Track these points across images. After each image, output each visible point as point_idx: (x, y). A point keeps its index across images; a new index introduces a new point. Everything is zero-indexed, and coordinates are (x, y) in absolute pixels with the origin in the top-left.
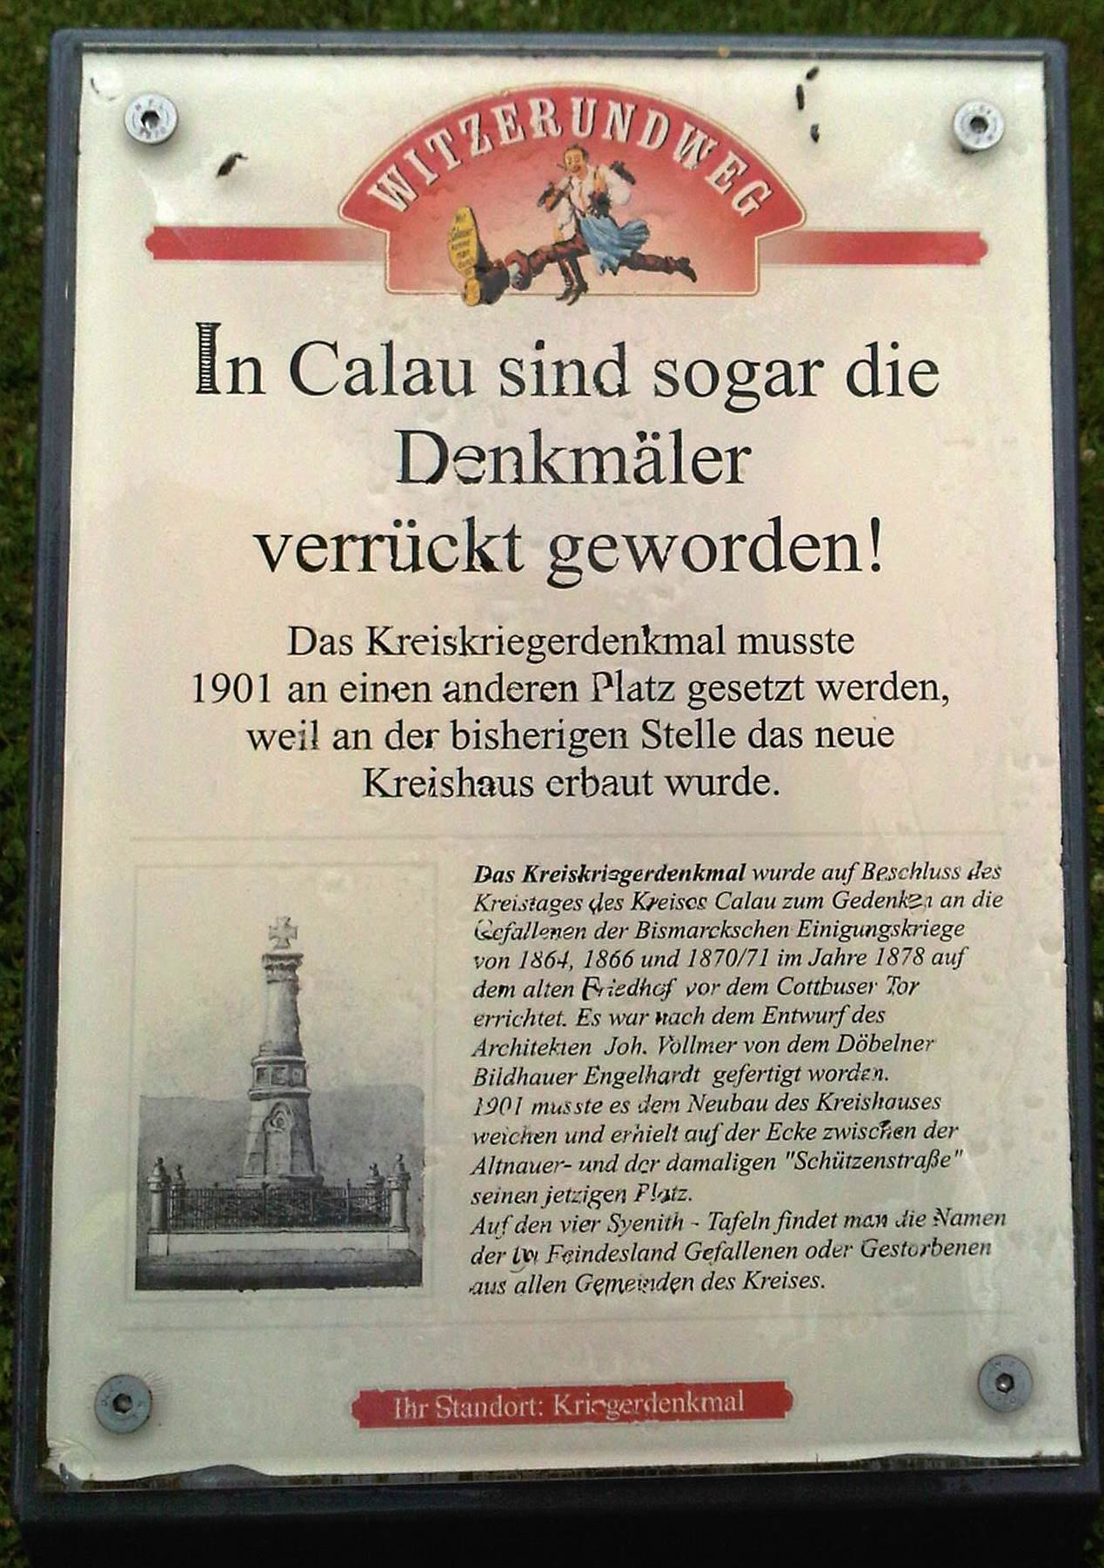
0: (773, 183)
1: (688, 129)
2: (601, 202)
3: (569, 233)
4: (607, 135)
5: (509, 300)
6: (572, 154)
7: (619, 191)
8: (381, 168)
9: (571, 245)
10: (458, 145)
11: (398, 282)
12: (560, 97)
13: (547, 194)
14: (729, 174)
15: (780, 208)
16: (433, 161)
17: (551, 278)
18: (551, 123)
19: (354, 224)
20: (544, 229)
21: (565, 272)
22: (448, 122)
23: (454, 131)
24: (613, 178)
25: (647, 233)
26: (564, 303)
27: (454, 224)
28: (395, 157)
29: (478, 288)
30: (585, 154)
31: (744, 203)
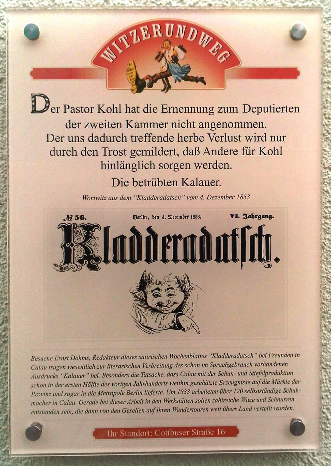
1: (203, 34)
2: (175, 59)
3: (165, 69)
5: (146, 91)
6: (166, 42)
7: (181, 55)
8: (104, 48)
9: (165, 73)
10: (129, 40)
11: (111, 85)
12: (162, 23)
14: (216, 49)
15: (233, 60)
16: (121, 45)
17: (160, 84)
18: (159, 33)
20: (156, 68)
22: (126, 32)
23: (128, 35)
24: (179, 51)
25: (190, 69)
26: (164, 92)
27: (128, 66)
28: (109, 44)
29: (136, 88)
30: (170, 43)
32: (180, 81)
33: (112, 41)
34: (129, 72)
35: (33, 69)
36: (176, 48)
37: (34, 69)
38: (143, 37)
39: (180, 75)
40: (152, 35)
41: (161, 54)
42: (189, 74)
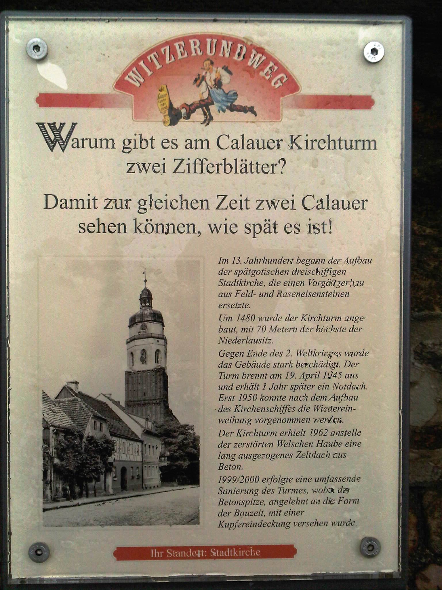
0: (289, 76)
2: (218, 84)
3: (206, 96)
4: (221, 55)
5: (182, 123)
7: (226, 78)
8: (130, 69)
9: (206, 101)
10: (161, 58)
11: (137, 116)
12: (202, 38)
13: (196, 80)
15: (291, 85)
16: (151, 65)
17: (198, 115)
18: (198, 50)
19: (118, 92)
21: (205, 114)
22: (156, 49)
24: (224, 73)
25: (237, 95)
28: (135, 64)
30: (212, 63)
31: (276, 83)
32: (224, 111)
33: (139, 59)
34: (160, 99)
35: (40, 94)
36: (220, 69)
37: (41, 95)
38: (177, 56)
39: (225, 104)
40: (189, 53)
41: (201, 76)
42: (236, 103)
